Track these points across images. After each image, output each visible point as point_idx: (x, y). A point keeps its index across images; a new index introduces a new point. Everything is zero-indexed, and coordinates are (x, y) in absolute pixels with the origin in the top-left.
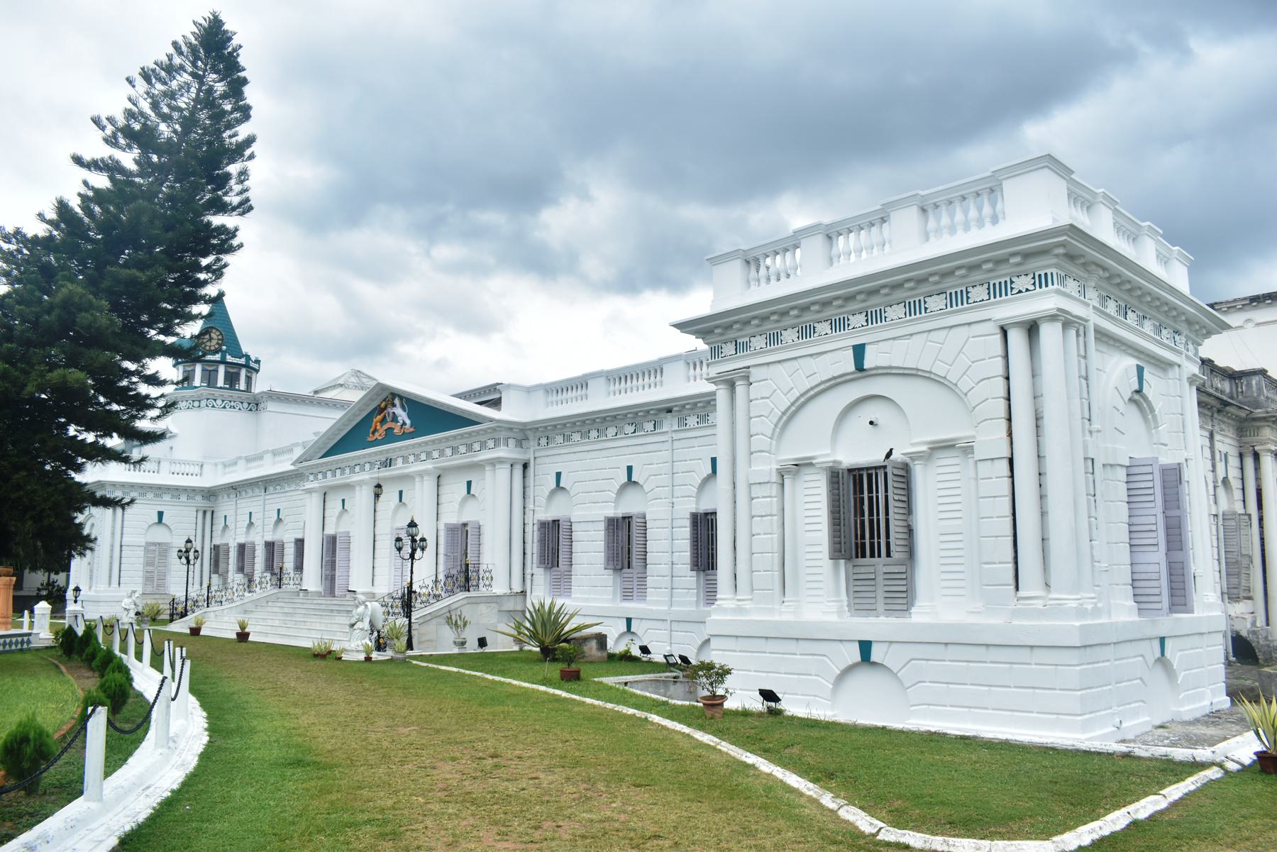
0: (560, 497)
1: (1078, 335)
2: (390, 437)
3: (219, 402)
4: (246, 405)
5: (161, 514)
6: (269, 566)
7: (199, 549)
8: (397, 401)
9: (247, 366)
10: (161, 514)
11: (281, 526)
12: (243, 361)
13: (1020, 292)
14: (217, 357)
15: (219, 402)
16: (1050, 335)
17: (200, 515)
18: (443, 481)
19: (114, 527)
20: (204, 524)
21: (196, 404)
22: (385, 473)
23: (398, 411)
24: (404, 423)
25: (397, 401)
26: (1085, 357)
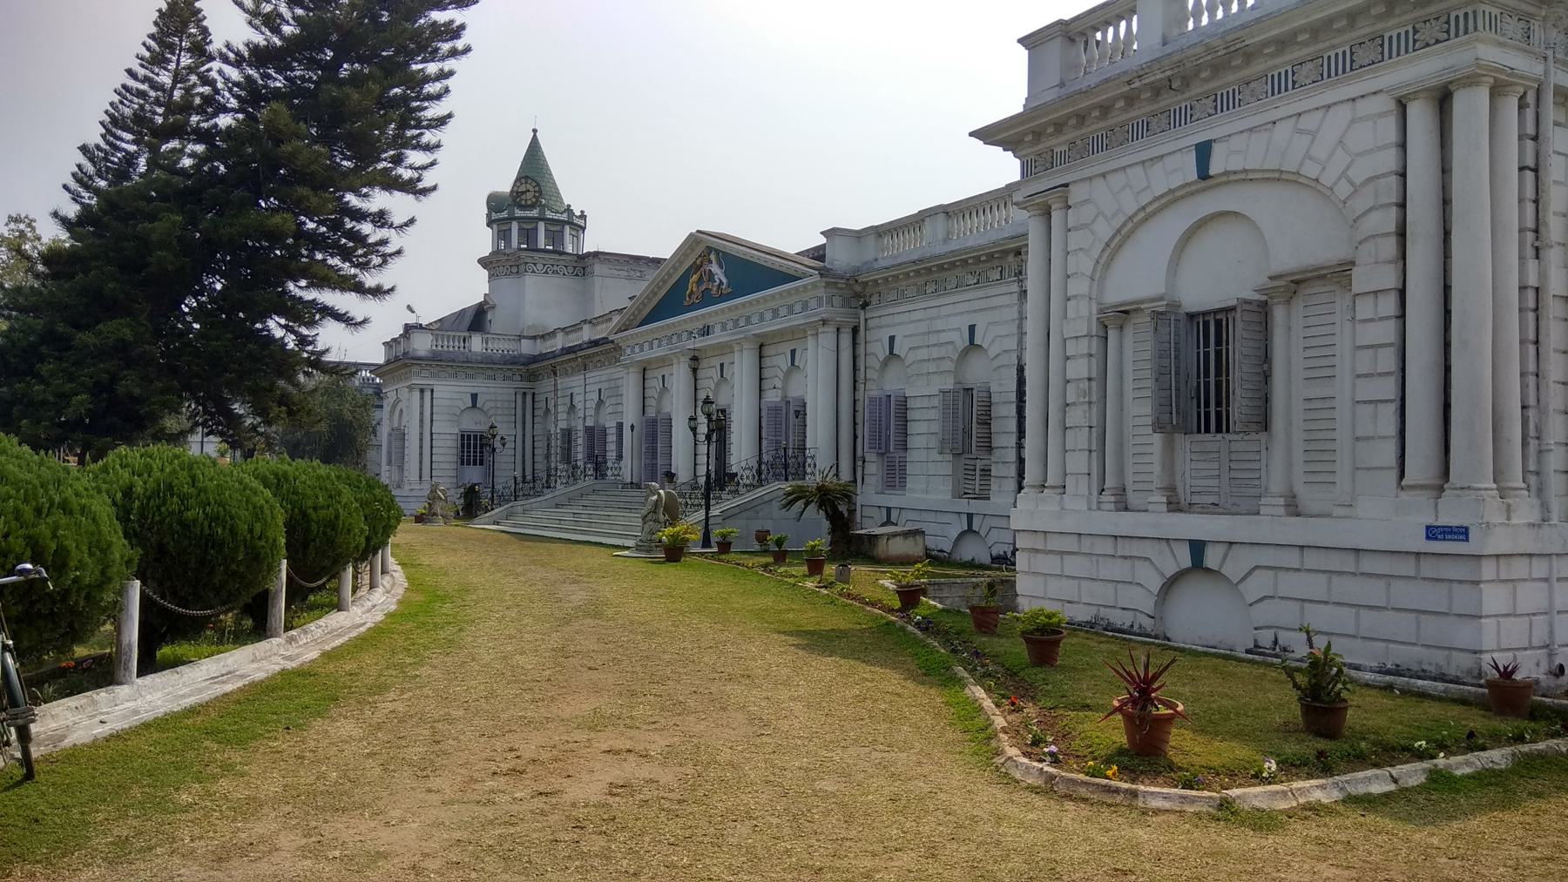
0: (894, 370)
1: (1522, 106)
2: (707, 299)
3: (540, 266)
8: (712, 257)
10: (474, 397)
13: (1428, 45)
16: (1471, 107)
17: (519, 398)
18: (767, 351)
19: (422, 413)
20: (524, 409)
22: (700, 343)
23: (715, 268)
25: (712, 257)
26: (1535, 138)
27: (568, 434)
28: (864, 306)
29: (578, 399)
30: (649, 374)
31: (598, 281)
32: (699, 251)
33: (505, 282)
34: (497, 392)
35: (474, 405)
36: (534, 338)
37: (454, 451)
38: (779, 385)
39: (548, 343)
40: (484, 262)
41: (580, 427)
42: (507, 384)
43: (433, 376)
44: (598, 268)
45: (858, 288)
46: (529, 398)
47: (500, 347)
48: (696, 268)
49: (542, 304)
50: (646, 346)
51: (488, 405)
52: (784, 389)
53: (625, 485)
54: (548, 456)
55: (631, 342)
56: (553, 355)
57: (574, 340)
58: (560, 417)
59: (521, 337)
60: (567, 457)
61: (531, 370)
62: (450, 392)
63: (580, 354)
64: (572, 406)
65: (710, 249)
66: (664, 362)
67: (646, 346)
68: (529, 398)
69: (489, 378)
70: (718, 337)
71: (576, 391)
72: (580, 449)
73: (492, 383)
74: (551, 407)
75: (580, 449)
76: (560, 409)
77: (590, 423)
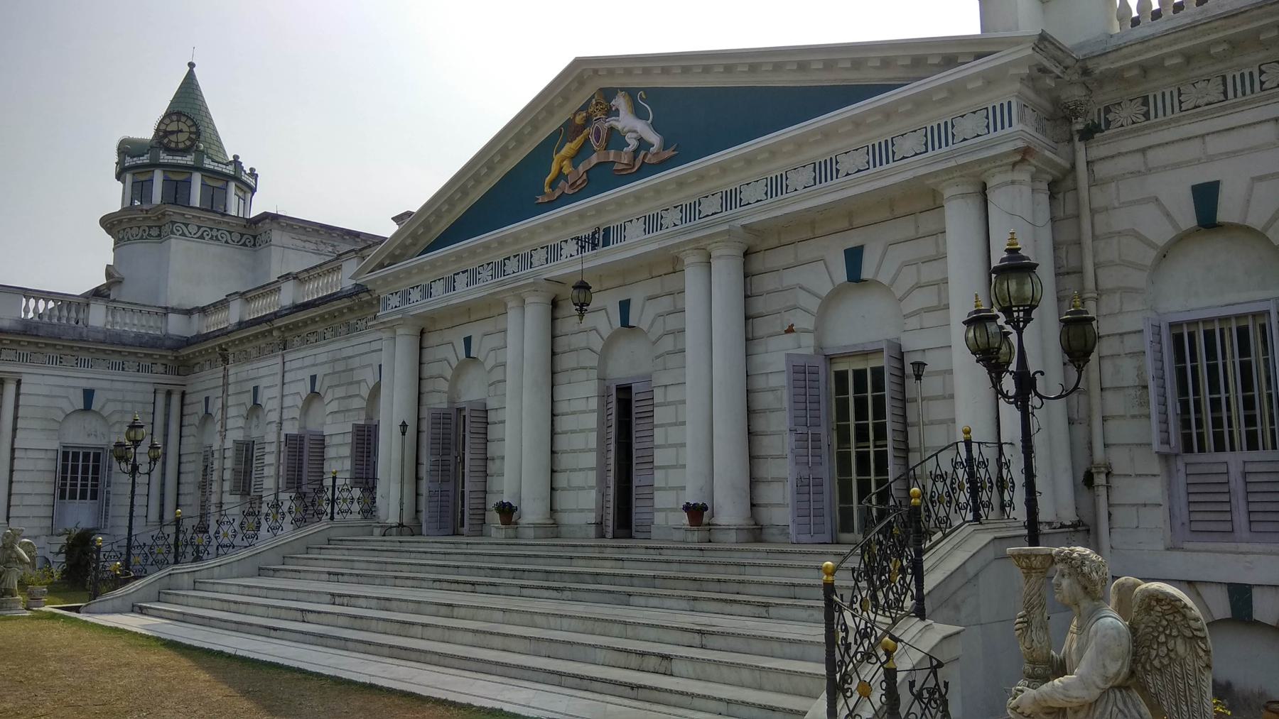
3: (193, 229)
4: (236, 237)
5: (88, 395)
6: (294, 480)
7: (158, 442)
8: (621, 102)
9: (236, 178)
10: (88, 395)
11: (316, 405)
12: (230, 170)
14: (189, 160)
15: (193, 229)
21: (154, 232)
23: (626, 121)
24: (643, 144)
25: (621, 102)
27: (247, 452)
28: (1088, 134)
29: (269, 398)
30: (431, 339)
31: (276, 253)
32: (579, 100)
33: (141, 251)
34: (126, 393)
35: (88, 407)
36: (189, 312)
37: (50, 477)
38: (803, 321)
39: (213, 319)
40: (109, 223)
41: (271, 436)
42: (145, 377)
43: (21, 359)
44: (277, 236)
45: (1075, 93)
46: (176, 399)
47: (131, 324)
48: (570, 130)
49: (195, 276)
50: (438, 288)
51: (110, 408)
52: (818, 331)
53: (386, 531)
54: (204, 486)
55: (402, 286)
56: (224, 332)
57: (262, 307)
58: (231, 423)
59: (167, 310)
60: (244, 482)
61: (180, 357)
62: (46, 387)
63: (279, 323)
64: (256, 406)
65: (608, 94)
66: (491, 308)
67: (438, 288)
68: (176, 399)
69: (113, 366)
70: (636, 243)
71: (263, 383)
72: (269, 471)
73: (118, 375)
74: (216, 408)
75: (269, 471)
76: (232, 412)
77: (291, 429)
